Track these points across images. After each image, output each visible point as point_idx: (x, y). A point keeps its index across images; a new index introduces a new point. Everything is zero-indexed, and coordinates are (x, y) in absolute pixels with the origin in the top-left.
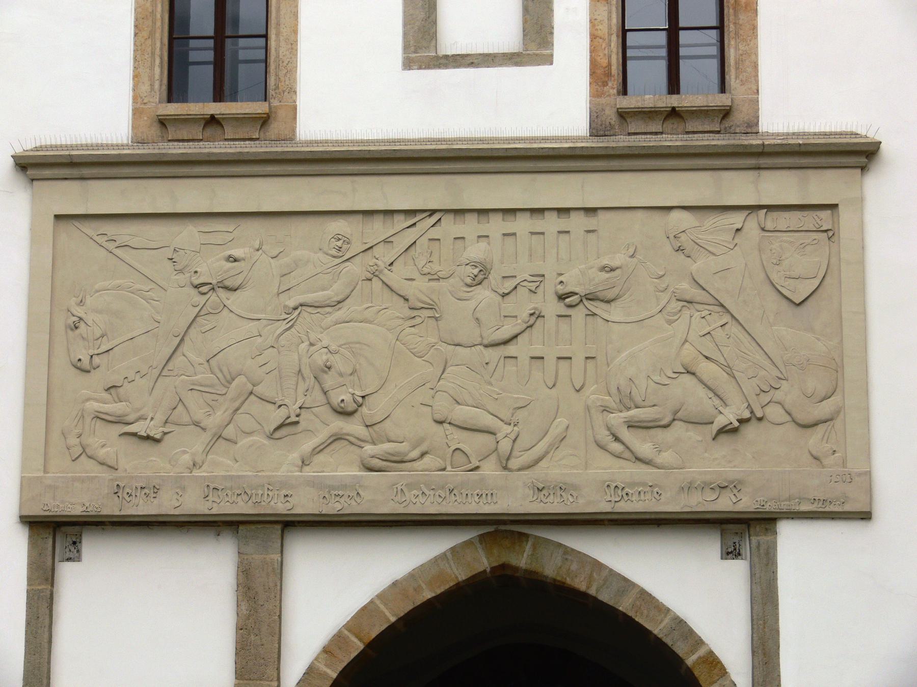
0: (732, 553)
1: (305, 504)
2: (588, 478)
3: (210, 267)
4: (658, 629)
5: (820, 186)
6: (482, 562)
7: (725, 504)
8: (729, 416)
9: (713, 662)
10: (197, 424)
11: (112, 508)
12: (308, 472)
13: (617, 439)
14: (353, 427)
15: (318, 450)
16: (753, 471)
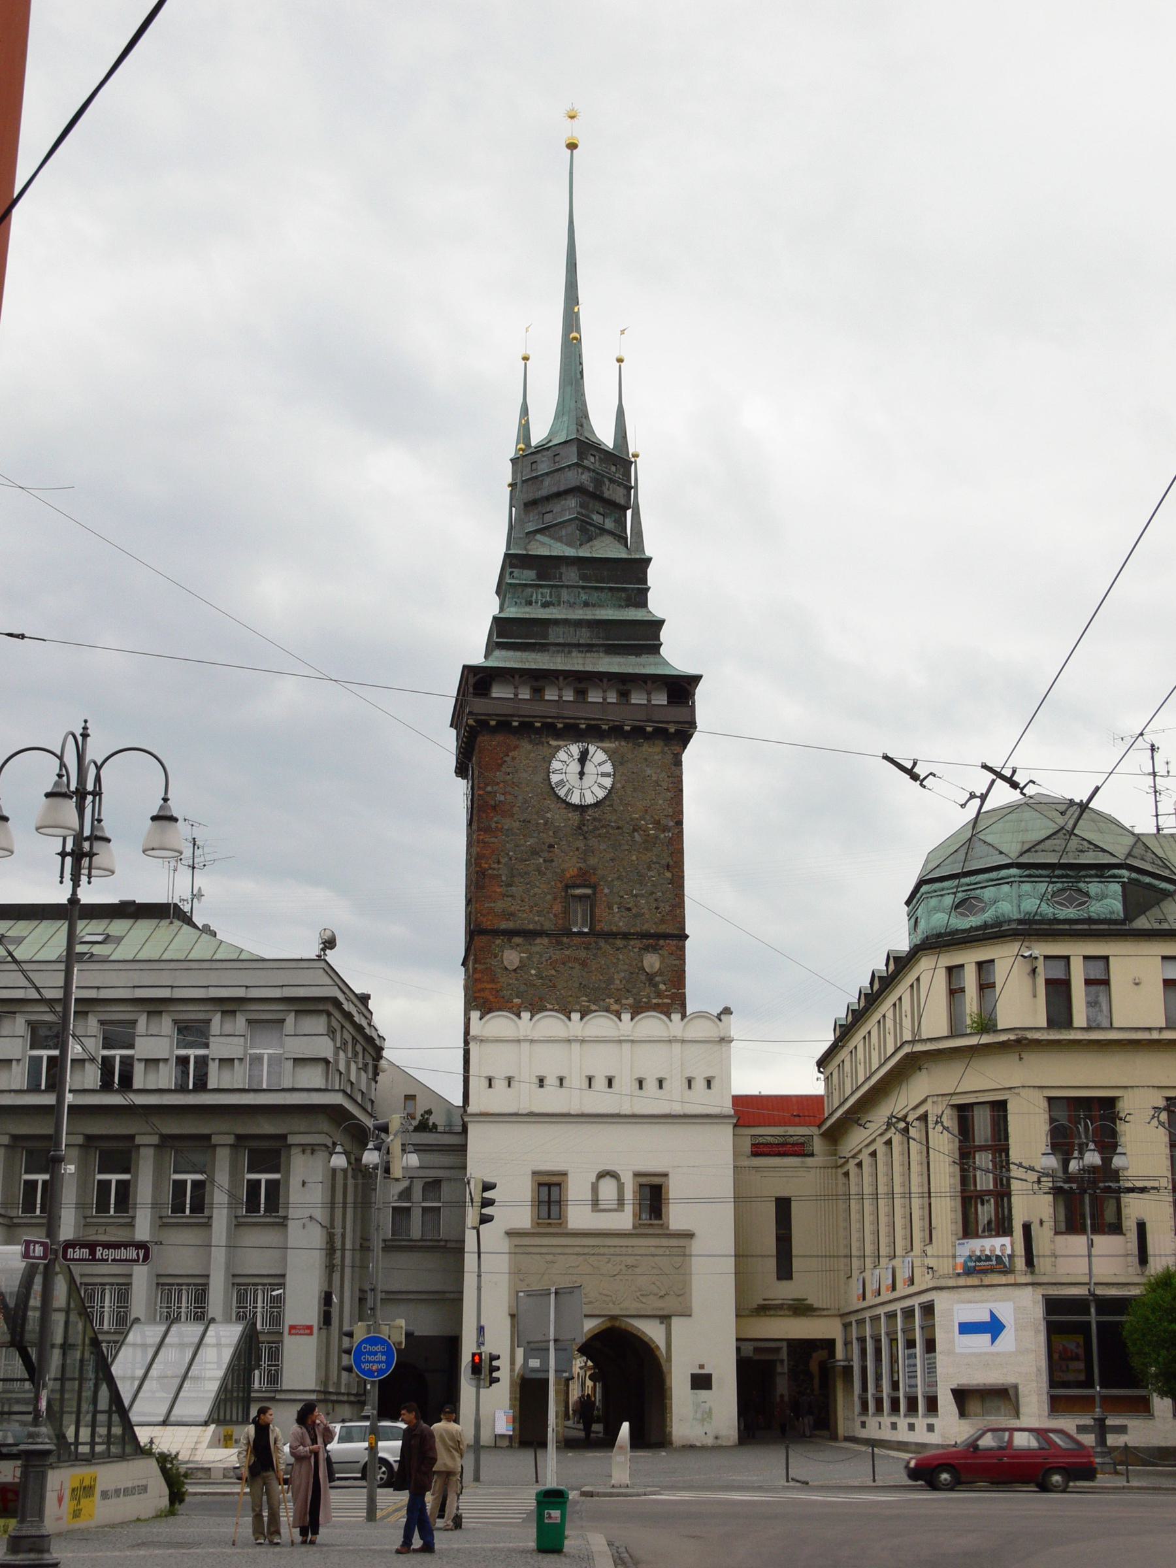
0: (662, 1323)
2: (632, 1307)
4: (646, 1339)
5: (682, 1242)
6: (609, 1325)
7: (661, 1313)
8: (662, 1293)
9: (657, 1347)
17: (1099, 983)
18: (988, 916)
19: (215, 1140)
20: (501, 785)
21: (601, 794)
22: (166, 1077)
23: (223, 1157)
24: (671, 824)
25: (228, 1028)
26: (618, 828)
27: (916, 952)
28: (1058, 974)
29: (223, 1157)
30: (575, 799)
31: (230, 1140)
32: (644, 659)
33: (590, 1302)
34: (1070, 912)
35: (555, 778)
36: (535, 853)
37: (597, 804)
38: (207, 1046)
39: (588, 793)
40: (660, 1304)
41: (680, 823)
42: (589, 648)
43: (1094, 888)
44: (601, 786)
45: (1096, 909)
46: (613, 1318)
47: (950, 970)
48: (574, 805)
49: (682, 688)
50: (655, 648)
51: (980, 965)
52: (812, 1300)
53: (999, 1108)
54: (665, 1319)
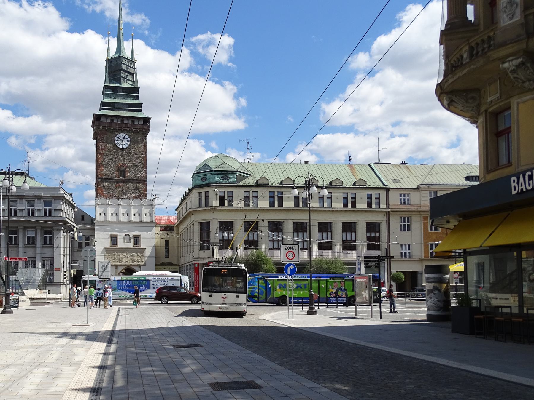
17: (231, 196)
18: (207, 182)
19: (36, 228)
21: (127, 146)
22: (25, 213)
23: (39, 232)
25: (39, 202)
27: (193, 188)
28: (222, 194)
29: (39, 232)
30: (121, 147)
31: (40, 228)
32: (138, 113)
34: (226, 181)
35: (116, 142)
37: (126, 148)
38: (34, 206)
41: (146, 153)
42: (125, 110)
43: (231, 176)
45: (230, 180)
46: (128, 266)
47: (199, 193)
49: (147, 120)
50: (140, 111)
51: (206, 192)
52: (173, 262)
53: (208, 223)
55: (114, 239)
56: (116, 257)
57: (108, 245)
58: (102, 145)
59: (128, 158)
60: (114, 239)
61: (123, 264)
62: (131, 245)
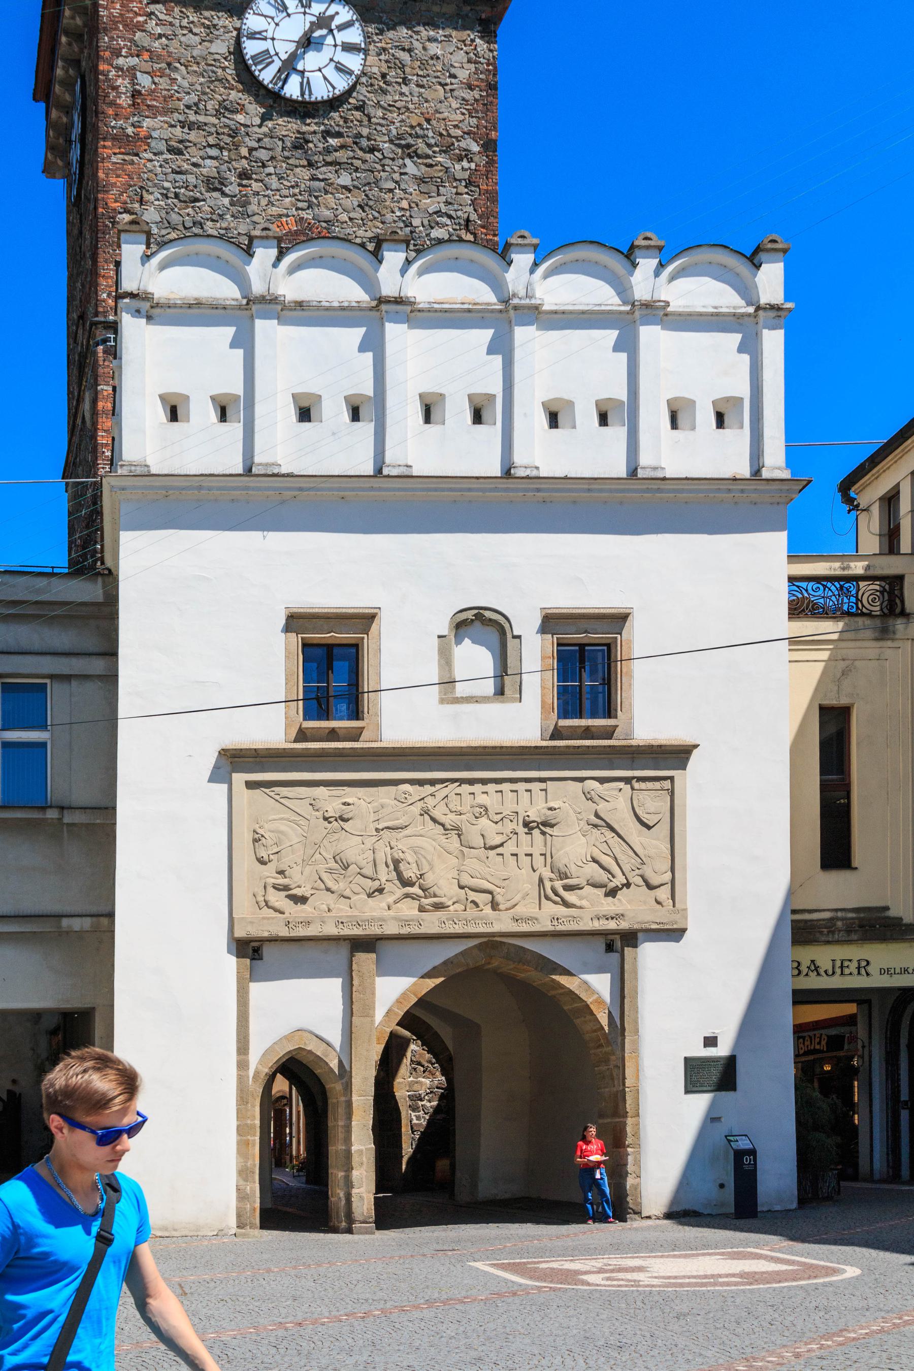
1: (392, 929)
3: (333, 808)
10: (328, 889)
11: (284, 932)
12: (391, 913)
13: (557, 894)
14: (415, 890)
15: (396, 902)
16: (634, 908)
20: (146, 56)
21: (341, 84)
24: (475, 148)
26: (372, 150)
33: (439, 907)
36: (216, 184)
37: (334, 103)
39: (316, 80)
40: (609, 906)
44: (341, 69)
48: (290, 101)
54: (618, 943)
55: (333, 662)
56: (354, 848)
57: (272, 728)
58: (131, 73)
59: (345, 179)
60: (333, 662)
61: (432, 924)
62: (524, 720)
